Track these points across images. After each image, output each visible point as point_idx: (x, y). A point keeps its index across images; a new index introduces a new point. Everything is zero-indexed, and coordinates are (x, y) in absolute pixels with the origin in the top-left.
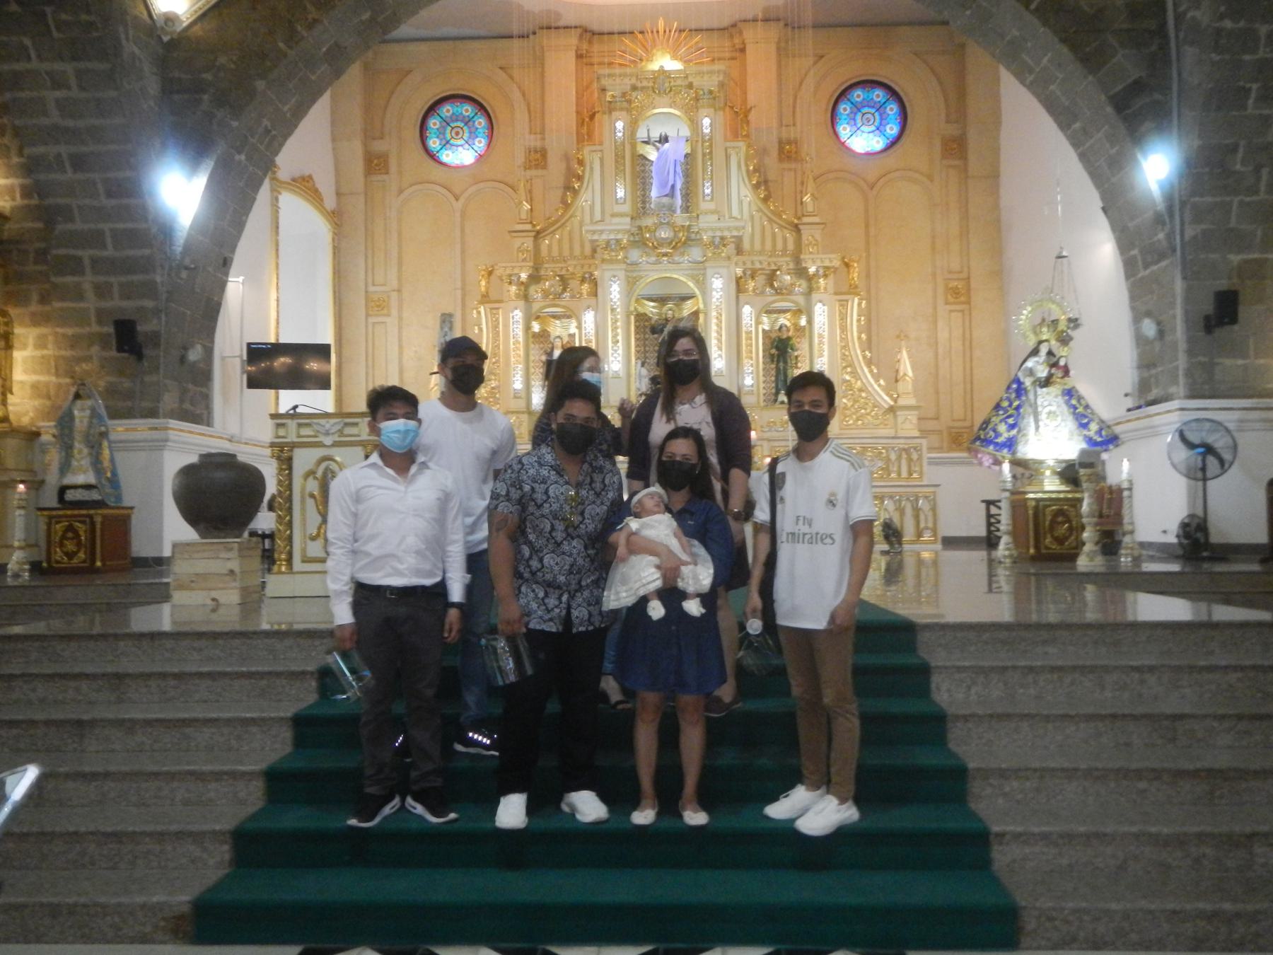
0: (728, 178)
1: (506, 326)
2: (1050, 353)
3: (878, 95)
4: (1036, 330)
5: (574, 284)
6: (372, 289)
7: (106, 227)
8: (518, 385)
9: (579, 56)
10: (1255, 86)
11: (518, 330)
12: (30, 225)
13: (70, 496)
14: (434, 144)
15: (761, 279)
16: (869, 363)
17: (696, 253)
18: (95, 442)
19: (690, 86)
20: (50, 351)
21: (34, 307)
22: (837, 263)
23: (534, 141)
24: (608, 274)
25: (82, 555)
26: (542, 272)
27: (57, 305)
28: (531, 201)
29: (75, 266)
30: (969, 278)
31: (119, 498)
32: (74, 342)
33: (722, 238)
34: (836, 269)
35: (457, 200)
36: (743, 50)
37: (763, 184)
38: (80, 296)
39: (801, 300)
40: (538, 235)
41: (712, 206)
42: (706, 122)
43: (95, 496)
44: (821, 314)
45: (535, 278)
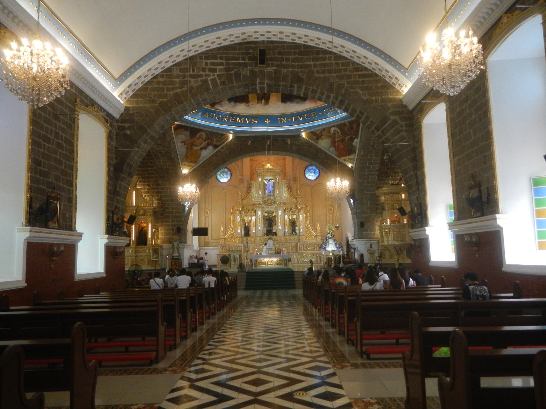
0: (282, 188)
1: (237, 219)
2: (331, 233)
3: (314, 167)
4: (329, 230)
5: (251, 211)
6: (205, 209)
7: (174, 210)
8: (239, 232)
9: (250, 159)
10: (365, 189)
11: (239, 220)
12: (159, 209)
13: (174, 258)
14: (218, 177)
15: (289, 210)
16: (313, 226)
17: (276, 205)
18: (178, 249)
19: (274, 171)
20: (163, 231)
21: (160, 224)
22: (304, 206)
23: (240, 177)
24: (258, 210)
25: (177, 267)
26: (244, 208)
27: (164, 223)
28: (241, 192)
29: (168, 217)
30: (333, 207)
31: (181, 258)
32: (167, 230)
33: (281, 203)
34: (304, 208)
35: (224, 190)
36: (285, 158)
37: (290, 188)
38: (168, 222)
39: (297, 214)
40: (243, 200)
41: (279, 196)
42: (277, 178)
43: (178, 257)
44: (301, 217)
45: (242, 209)
